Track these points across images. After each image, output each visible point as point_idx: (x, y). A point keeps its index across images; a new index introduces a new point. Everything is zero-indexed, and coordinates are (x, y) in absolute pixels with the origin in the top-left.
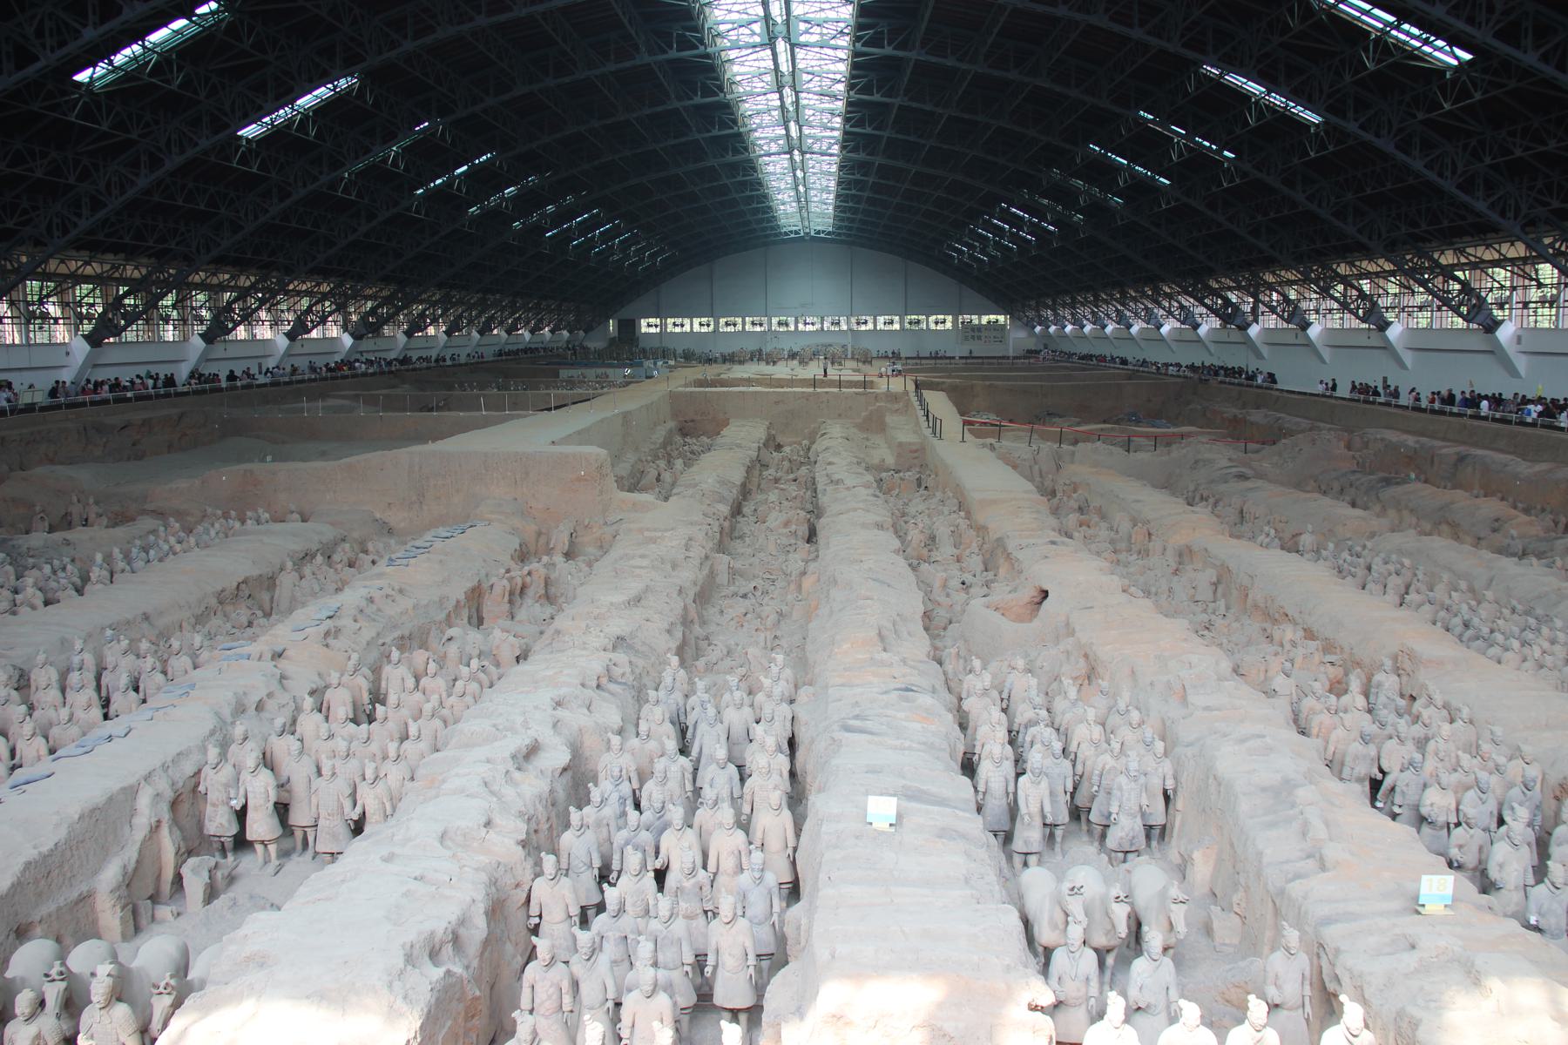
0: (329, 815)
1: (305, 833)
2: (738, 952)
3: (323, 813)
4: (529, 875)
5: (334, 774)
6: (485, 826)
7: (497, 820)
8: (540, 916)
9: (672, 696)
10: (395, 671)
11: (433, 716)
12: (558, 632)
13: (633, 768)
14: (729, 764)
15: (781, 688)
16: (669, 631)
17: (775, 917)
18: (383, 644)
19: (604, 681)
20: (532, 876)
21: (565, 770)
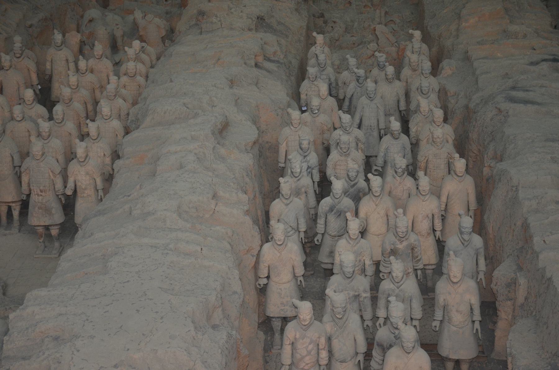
0: (41, 191)
1: (10, 208)
2: (465, 308)
3: (35, 190)
4: (257, 241)
5: (43, 154)
6: (213, 199)
7: (221, 193)
8: (268, 277)
9: (324, 73)
10: (60, 52)
11: (115, 96)
12: (202, 13)
13: (312, 140)
14: (402, 135)
15: (427, 65)
16: (296, 10)
17: (481, 276)
18: (31, 26)
19: (260, 59)
20: (260, 242)
21: (255, 143)
